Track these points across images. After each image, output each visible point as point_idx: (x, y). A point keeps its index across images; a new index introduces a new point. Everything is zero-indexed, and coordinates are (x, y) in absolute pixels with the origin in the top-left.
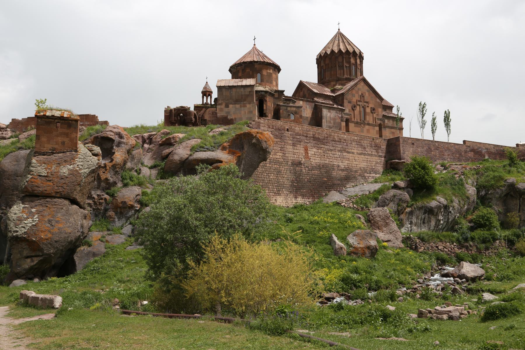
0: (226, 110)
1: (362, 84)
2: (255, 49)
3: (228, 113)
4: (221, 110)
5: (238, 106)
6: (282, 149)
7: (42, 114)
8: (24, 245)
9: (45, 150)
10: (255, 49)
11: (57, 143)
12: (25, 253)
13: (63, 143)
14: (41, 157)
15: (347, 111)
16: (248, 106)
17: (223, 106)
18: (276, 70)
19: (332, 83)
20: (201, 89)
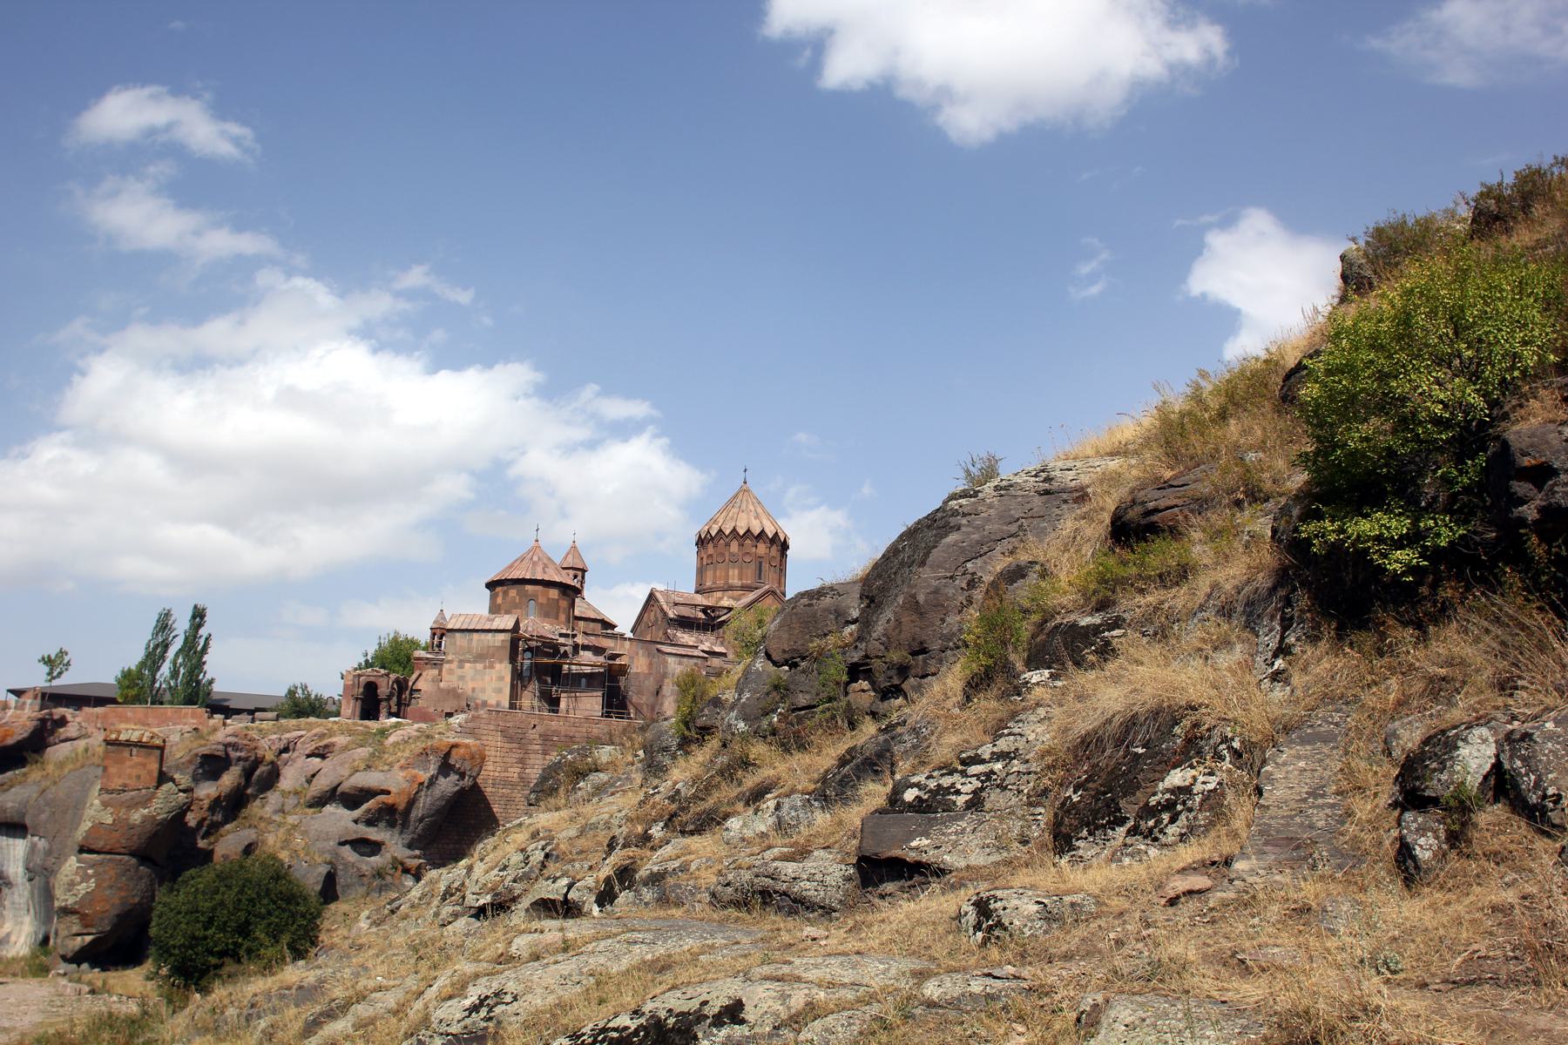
0: (459, 672)
1: (769, 600)
2: (536, 548)
3: (462, 678)
4: (451, 672)
5: (479, 666)
6: (522, 761)
7: (113, 736)
8: (74, 919)
9: (113, 786)
10: (536, 548)
11: (130, 777)
12: (75, 929)
13: (139, 777)
14: (106, 797)
15: (731, 656)
16: (498, 666)
17: (454, 666)
18: (570, 593)
19: (719, 594)
20: (430, 624)
